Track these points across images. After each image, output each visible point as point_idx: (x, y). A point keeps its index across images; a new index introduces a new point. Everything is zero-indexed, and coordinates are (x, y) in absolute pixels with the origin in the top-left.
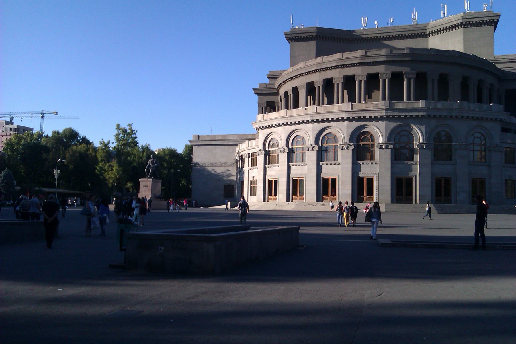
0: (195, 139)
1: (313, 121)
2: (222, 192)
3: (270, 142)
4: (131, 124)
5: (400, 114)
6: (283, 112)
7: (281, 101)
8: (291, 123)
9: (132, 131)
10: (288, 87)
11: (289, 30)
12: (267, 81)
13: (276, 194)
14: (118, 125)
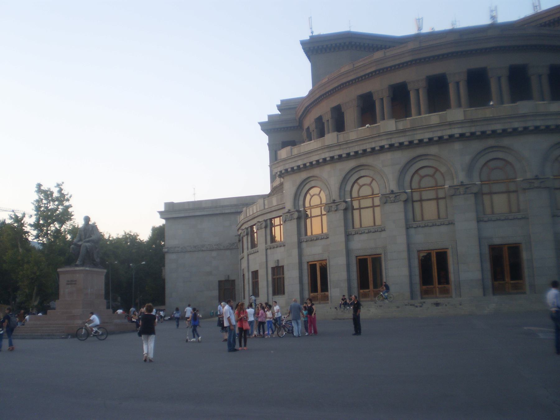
1: (392, 147)
2: (216, 293)
4: (60, 182)
6: (331, 138)
8: (348, 154)
9: (63, 195)
10: (324, 109)
11: (307, 37)
12: (279, 113)
13: (325, 287)
14: (39, 186)
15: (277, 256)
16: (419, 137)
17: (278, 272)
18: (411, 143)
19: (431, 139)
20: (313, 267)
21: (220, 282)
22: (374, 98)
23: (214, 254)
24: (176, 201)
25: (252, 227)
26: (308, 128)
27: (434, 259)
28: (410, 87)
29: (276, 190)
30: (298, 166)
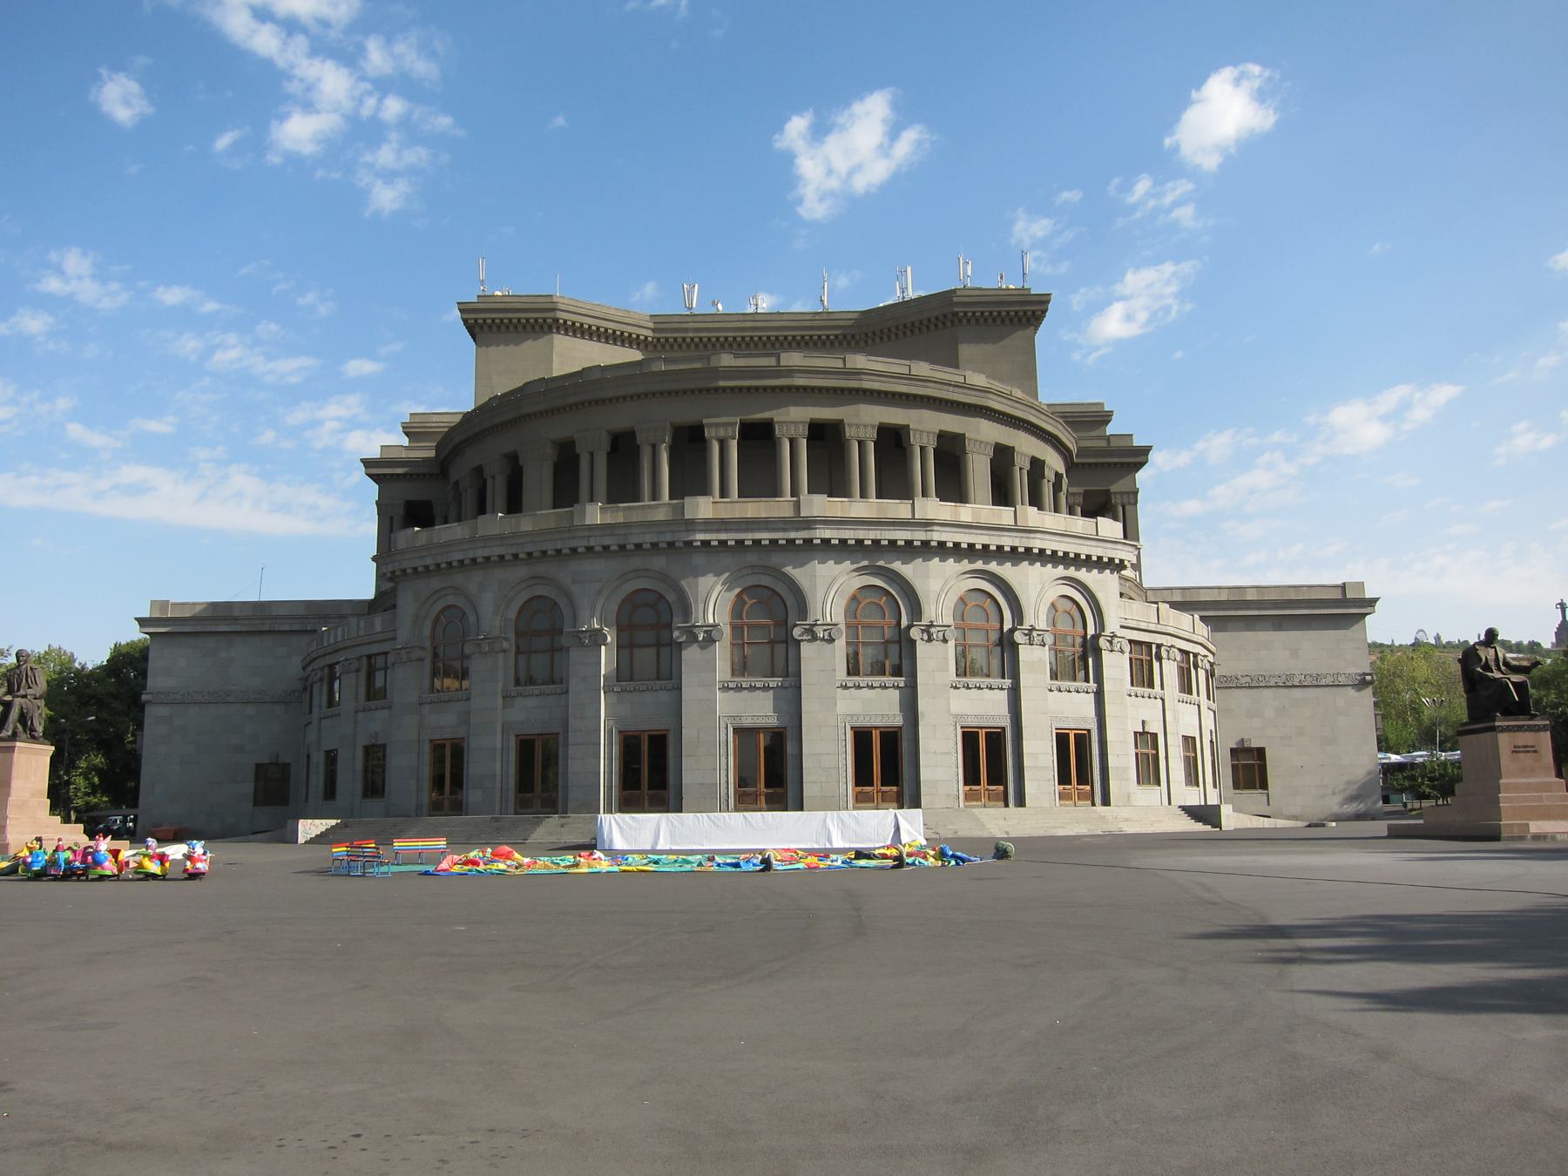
0: (157, 615)
2: (249, 788)
3: (438, 617)
5: (861, 534)
7: (458, 497)
10: (489, 456)
12: (405, 441)
15: (374, 725)
16: (637, 540)
17: (375, 755)
18: (622, 547)
19: (654, 545)
20: (438, 748)
21: (259, 767)
22: (578, 450)
23: (250, 710)
24: (175, 598)
25: (331, 666)
26: (457, 483)
27: (645, 746)
28: (640, 438)
29: (384, 601)
30: (427, 567)
